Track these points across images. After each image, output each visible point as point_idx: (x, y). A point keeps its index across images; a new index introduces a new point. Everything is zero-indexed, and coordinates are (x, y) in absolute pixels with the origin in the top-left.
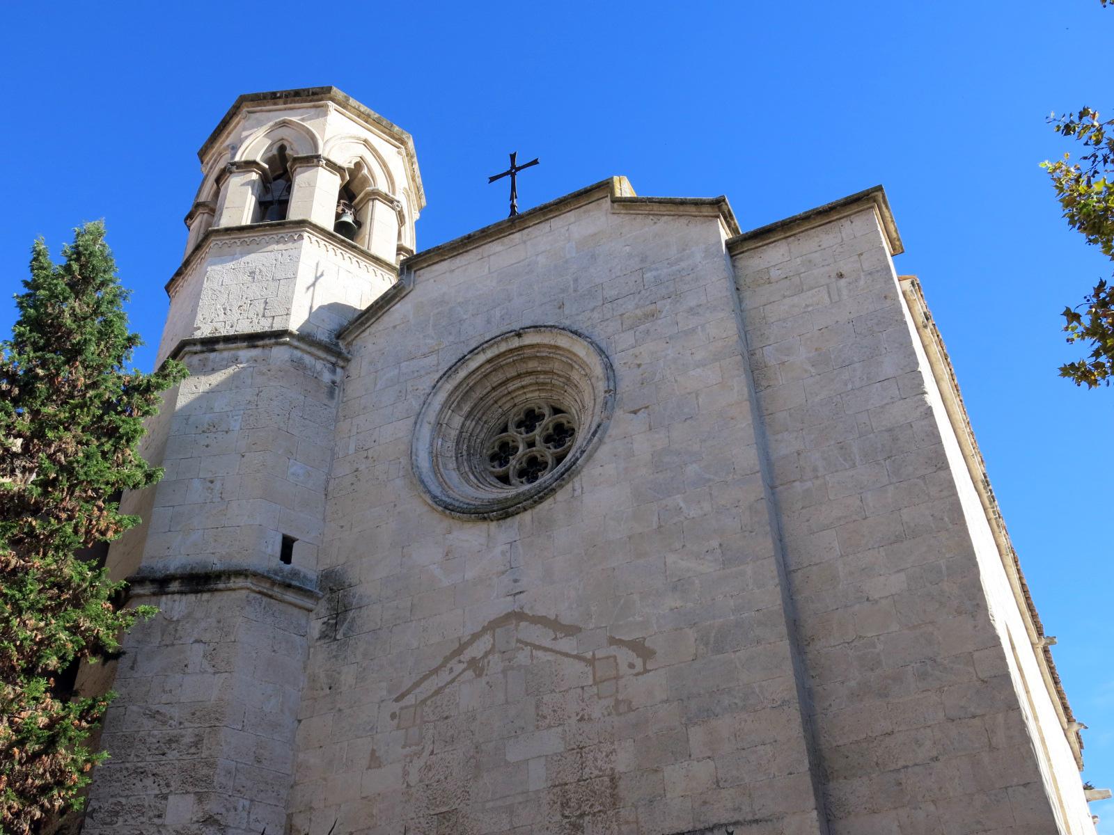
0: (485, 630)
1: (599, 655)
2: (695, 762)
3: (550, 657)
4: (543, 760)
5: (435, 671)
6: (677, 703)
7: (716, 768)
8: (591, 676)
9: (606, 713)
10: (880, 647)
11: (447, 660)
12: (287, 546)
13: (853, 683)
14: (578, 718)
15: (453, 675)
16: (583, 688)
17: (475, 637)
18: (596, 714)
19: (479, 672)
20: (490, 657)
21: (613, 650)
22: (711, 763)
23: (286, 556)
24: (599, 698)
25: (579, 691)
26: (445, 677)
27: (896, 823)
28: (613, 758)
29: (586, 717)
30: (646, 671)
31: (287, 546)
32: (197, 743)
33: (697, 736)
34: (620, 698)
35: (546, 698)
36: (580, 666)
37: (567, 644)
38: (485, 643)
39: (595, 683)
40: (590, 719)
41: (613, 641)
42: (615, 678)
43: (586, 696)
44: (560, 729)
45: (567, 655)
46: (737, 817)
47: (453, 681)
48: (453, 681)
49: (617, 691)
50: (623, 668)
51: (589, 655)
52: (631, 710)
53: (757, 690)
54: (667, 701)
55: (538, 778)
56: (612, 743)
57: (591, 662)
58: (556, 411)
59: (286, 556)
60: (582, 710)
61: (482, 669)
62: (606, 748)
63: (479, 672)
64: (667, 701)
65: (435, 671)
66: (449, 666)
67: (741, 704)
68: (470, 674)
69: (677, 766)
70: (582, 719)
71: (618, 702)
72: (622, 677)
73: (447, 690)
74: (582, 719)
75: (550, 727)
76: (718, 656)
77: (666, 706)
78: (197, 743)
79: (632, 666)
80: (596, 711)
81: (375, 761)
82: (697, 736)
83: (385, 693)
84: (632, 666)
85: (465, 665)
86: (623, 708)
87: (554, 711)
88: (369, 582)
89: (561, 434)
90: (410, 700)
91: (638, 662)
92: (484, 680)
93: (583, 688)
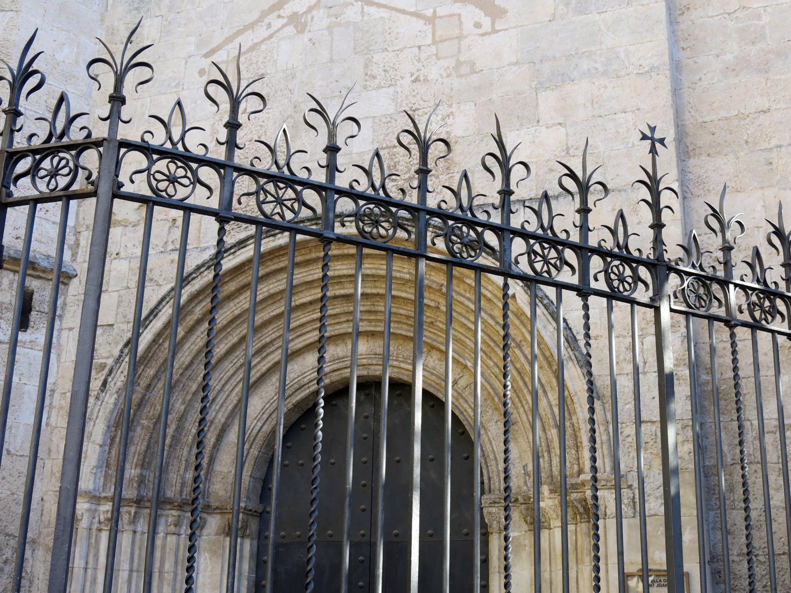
1: (441, 12)
2: (544, 128)
4: (371, 120)
5: (251, 26)
6: (526, 66)
7: (567, 135)
8: (430, 36)
9: (445, 75)
10: (766, 19)
11: (264, 14)
14: (413, 78)
15: (271, 31)
16: (419, 47)
18: (433, 75)
20: (314, 12)
22: (563, 130)
24: (438, 59)
25: (416, 50)
26: (261, 32)
27: (761, 203)
28: (450, 121)
29: (422, 78)
30: (494, 31)
34: (462, 59)
35: (377, 57)
36: (419, 24)
39: (434, 42)
40: (426, 80)
42: (457, 38)
43: (423, 56)
44: (391, 89)
45: (403, 12)
47: (271, 36)
48: (271, 36)
49: (459, 52)
50: (468, 26)
51: (429, 13)
52: (473, 72)
53: (622, 55)
54: (516, 63)
56: (450, 106)
57: (431, 20)
60: (418, 70)
61: (304, 26)
62: (442, 110)
64: (516, 63)
65: (251, 26)
66: (266, 21)
67: (601, 69)
68: (290, 30)
69: (523, 132)
70: (417, 80)
71: (459, 64)
72: (466, 37)
73: (263, 47)
74: (417, 80)
75: (379, 87)
76: (581, 17)
77: (515, 68)
79: (478, 25)
80: (434, 72)
82: (548, 101)
83: (192, 48)
84: (478, 25)
85: (285, 21)
86: (464, 69)
87: (385, 71)
91: (486, 22)
92: (306, 36)
93: (419, 47)
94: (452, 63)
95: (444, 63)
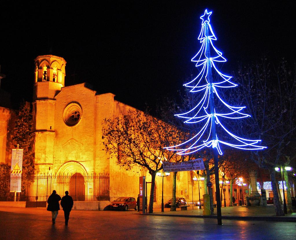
0: (70, 139)
3: (75, 143)
12: (51, 127)
17: (69, 140)
19: (69, 144)
21: (80, 144)
23: (51, 128)
31: (51, 127)
32: (44, 149)
36: (78, 145)
37: (77, 143)
38: (70, 141)
41: (81, 143)
55: (74, 155)
57: (79, 145)
58: (79, 112)
59: (51, 128)
63: (69, 144)
65: (65, 143)
68: (68, 144)
78: (44, 149)
81: (61, 151)
88: (59, 131)
89: (79, 115)
90: (63, 146)
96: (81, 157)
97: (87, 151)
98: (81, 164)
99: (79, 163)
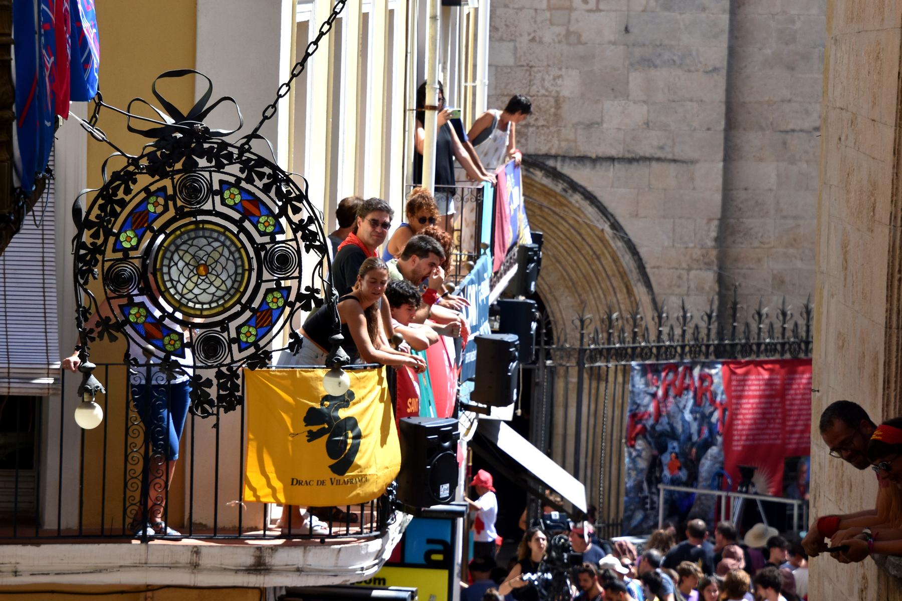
2: (632, 103)
6: (622, 47)
7: (648, 111)
9: (556, 40)
10: (798, 25)
13: (768, 52)
14: (530, 38)
16: (536, 10)
22: (645, 107)
24: (552, 24)
25: (532, 12)
28: (559, 82)
29: (537, 39)
30: (598, 10)
33: (636, 79)
34: (572, 29)
39: (549, 8)
40: (541, 42)
42: (567, 9)
43: (539, 19)
46: (659, 154)
49: (569, 22)
52: (580, 42)
53: (694, 53)
54: (614, 43)
56: (560, 69)
60: (535, 31)
62: (554, 71)
64: (614, 43)
67: (678, 62)
69: (616, 102)
70: (533, 40)
71: (568, 34)
72: (575, 9)
74: (533, 40)
76: (666, 13)
77: (613, 47)
80: (548, 35)
82: (636, 79)
86: (573, 39)
87: (507, 26)
93: (536, 10)
94: (562, 30)
95: (557, 29)
96: (571, 114)
97: (648, 63)
98: (574, 187)
99: (555, 175)
